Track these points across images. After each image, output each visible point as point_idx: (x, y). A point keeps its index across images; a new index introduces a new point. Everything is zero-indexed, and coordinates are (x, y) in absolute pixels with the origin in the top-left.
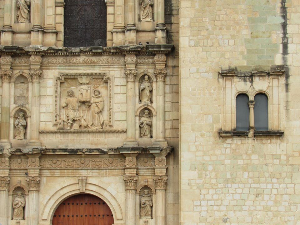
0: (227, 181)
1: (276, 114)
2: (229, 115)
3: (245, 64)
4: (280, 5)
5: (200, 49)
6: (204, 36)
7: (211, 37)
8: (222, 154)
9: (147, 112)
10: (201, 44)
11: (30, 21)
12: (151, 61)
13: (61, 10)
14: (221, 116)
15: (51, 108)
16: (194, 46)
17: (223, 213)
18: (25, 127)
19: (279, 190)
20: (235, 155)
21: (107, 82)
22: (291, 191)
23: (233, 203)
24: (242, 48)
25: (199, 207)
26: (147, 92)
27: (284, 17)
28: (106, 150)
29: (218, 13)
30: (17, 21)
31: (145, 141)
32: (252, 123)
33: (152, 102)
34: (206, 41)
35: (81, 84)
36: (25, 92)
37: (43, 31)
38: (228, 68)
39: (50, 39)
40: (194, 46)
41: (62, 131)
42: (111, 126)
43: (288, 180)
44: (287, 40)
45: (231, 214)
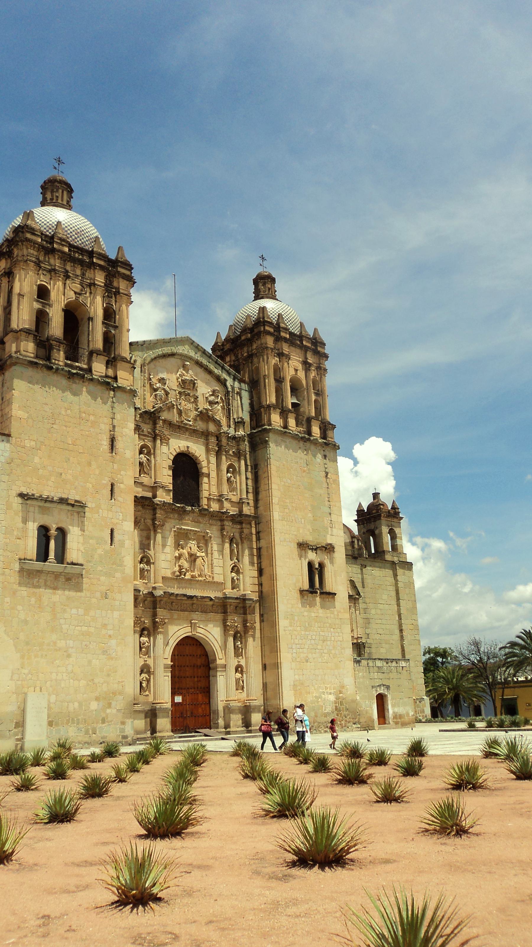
1: (330, 579)
4: (327, 499)
7: (291, 515)
10: (286, 519)
11: (151, 478)
12: (239, 527)
13: (170, 473)
17: (305, 655)
23: (311, 647)
24: (309, 527)
36: (144, 539)
42: (213, 578)
43: (339, 630)
45: (310, 656)
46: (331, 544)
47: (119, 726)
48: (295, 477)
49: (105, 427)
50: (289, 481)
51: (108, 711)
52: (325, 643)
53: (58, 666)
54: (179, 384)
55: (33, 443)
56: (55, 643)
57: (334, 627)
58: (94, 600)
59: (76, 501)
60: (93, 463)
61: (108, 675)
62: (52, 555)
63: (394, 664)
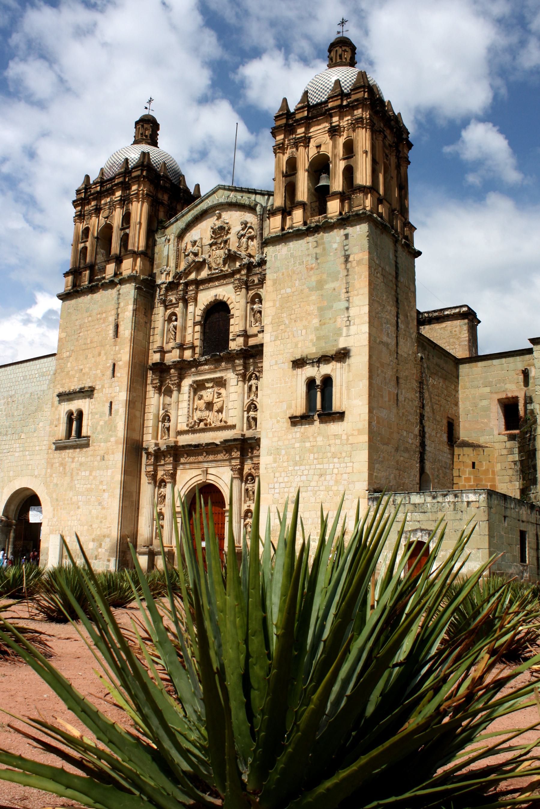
0: (296, 464)
1: (338, 395)
2: (299, 400)
3: (314, 351)
5: (278, 342)
6: (282, 330)
7: (288, 330)
8: (293, 438)
9: (252, 407)
13: (198, 328)
14: (293, 402)
15: (186, 410)
16: (275, 341)
18: (168, 429)
19: (339, 469)
20: (304, 439)
21: (225, 385)
22: (349, 470)
24: (313, 337)
25: (273, 490)
26: (254, 389)
27: (348, 301)
28: (219, 443)
29: (294, 307)
30: (167, 343)
31: (249, 434)
32: (319, 406)
33: (257, 397)
34: (283, 334)
35: (208, 388)
37: (182, 347)
38: (299, 357)
39: (188, 354)
40: (275, 341)
41: (192, 430)
42: (226, 422)
43: (347, 459)
44: (350, 321)
46: (345, 349)
47: (106, 563)
48: (297, 282)
49: (112, 319)
50: (289, 290)
51: (100, 550)
52: (323, 478)
53: (72, 516)
54: (212, 237)
55: (68, 353)
56: (71, 498)
57: (339, 455)
58: (96, 463)
59: (90, 387)
60: (103, 352)
61: (101, 522)
62: (73, 433)
63: (450, 498)
